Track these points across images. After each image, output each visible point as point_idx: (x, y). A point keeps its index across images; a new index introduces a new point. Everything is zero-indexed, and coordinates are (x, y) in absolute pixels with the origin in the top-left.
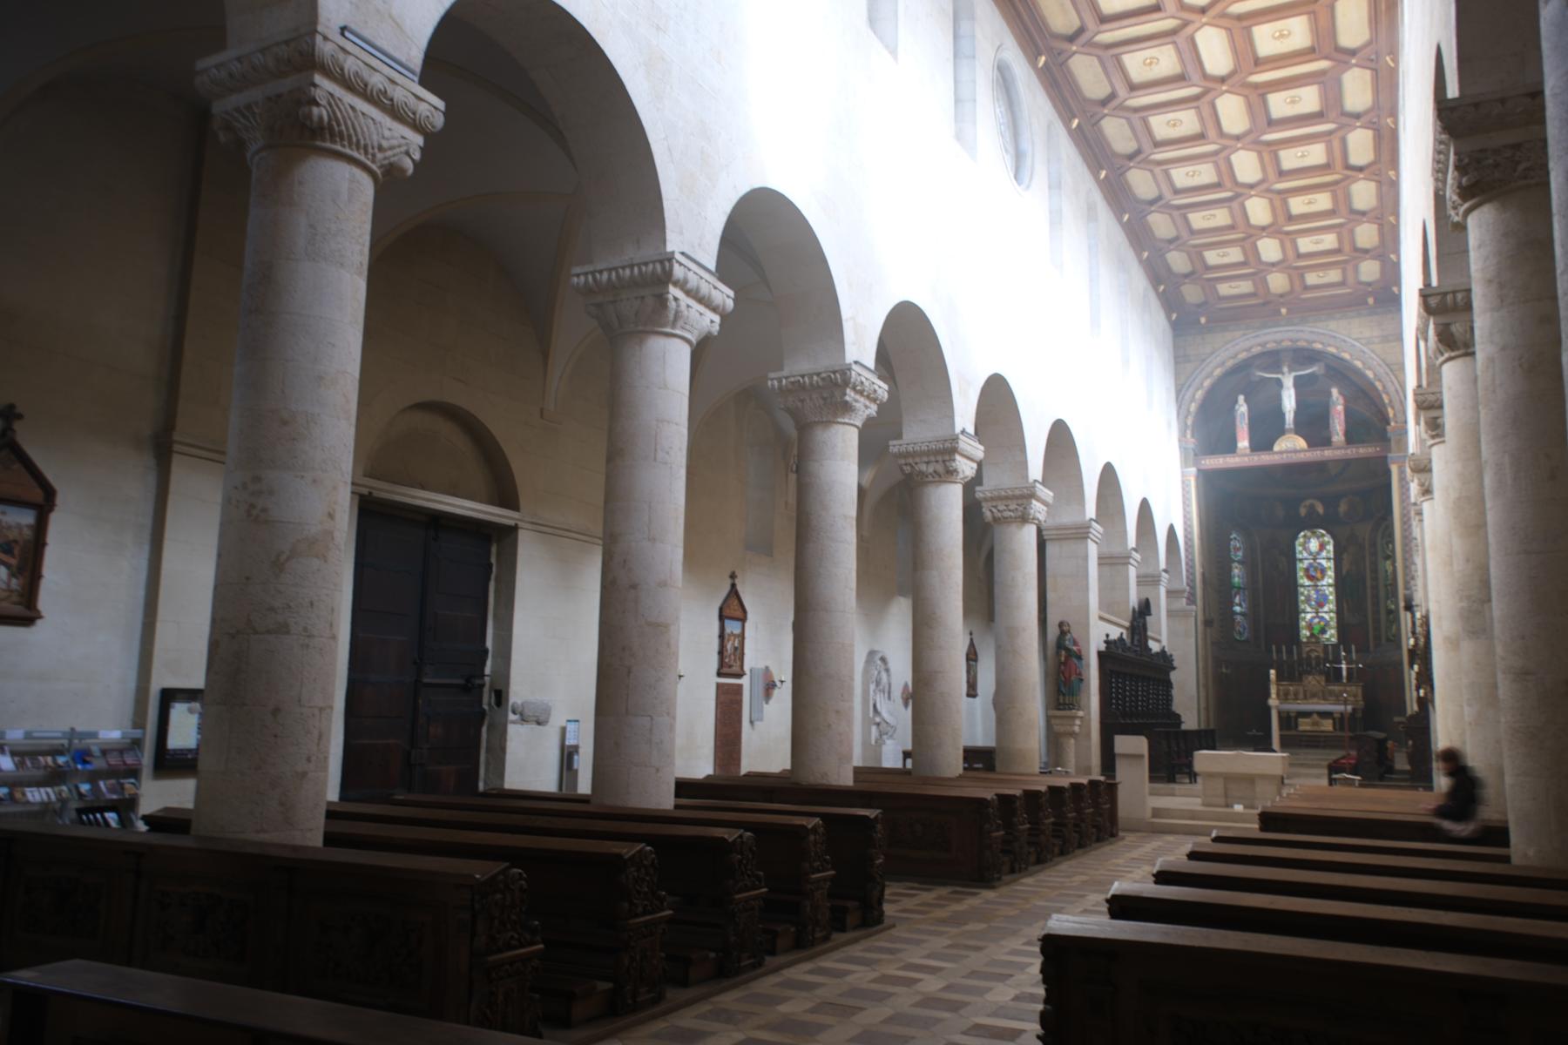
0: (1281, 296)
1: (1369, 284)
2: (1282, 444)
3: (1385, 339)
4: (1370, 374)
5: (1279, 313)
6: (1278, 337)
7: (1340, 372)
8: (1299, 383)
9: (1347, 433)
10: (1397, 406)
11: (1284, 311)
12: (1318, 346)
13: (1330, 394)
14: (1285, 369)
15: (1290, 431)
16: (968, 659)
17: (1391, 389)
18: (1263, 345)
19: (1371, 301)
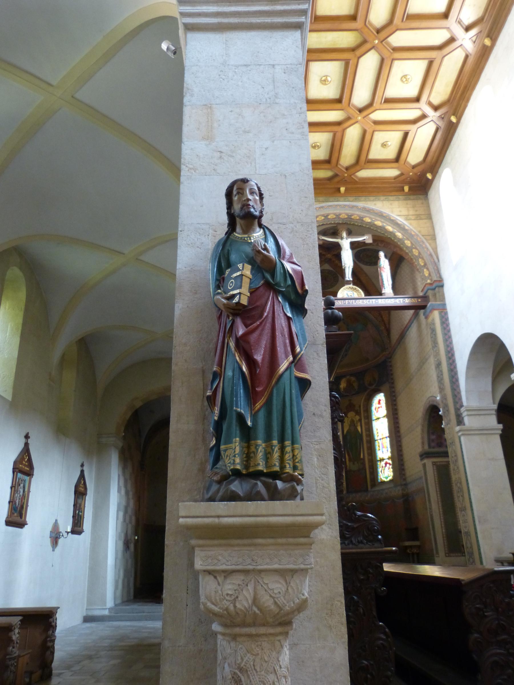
0: (347, 169)
1: (414, 167)
2: (344, 292)
3: (418, 217)
4: (408, 243)
5: (339, 190)
6: (337, 212)
7: (383, 241)
8: (353, 245)
9: (394, 288)
10: (430, 267)
11: (343, 189)
12: (368, 220)
13: (378, 258)
14: (344, 234)
15: (348, 282)
16: (16, 469)
17: (425, 255)
18: (326, 216)
19: (406, 189)
